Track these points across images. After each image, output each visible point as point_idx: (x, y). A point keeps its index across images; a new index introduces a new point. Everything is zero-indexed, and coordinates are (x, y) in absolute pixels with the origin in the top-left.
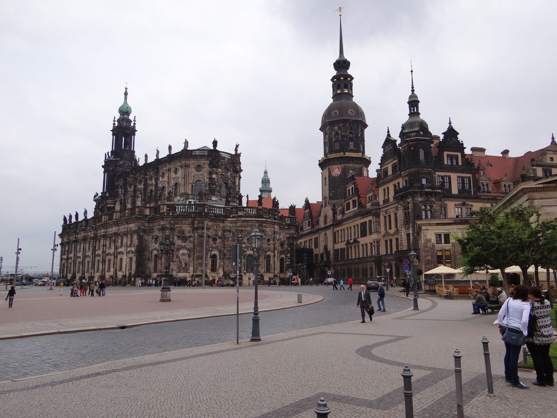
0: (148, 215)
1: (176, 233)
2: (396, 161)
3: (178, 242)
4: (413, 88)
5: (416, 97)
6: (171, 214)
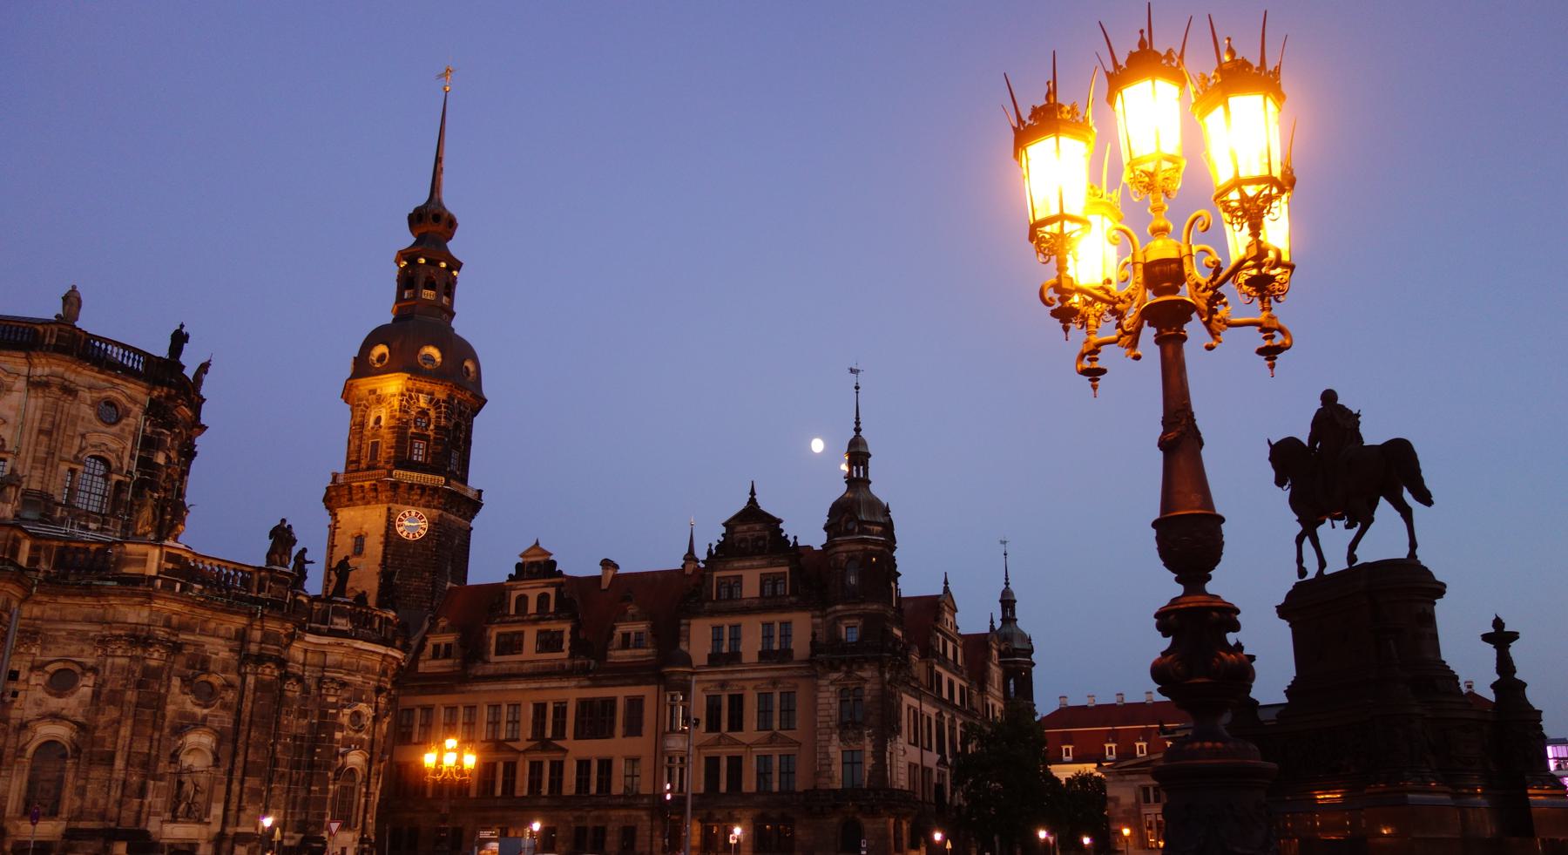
0: (21, 568)
1: (179, 663)
2: (786, 569)
3: (180, 701)
4: (857, 423)
5: (865, 444)
6: (178, 586)
